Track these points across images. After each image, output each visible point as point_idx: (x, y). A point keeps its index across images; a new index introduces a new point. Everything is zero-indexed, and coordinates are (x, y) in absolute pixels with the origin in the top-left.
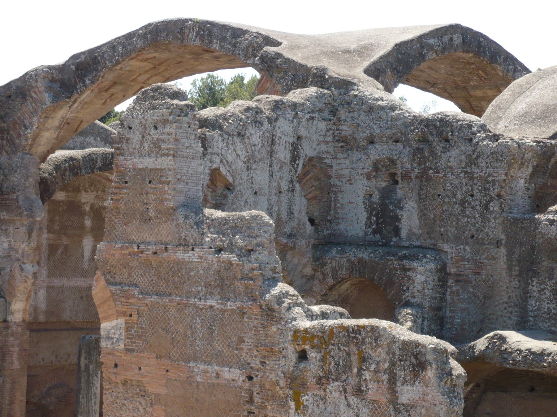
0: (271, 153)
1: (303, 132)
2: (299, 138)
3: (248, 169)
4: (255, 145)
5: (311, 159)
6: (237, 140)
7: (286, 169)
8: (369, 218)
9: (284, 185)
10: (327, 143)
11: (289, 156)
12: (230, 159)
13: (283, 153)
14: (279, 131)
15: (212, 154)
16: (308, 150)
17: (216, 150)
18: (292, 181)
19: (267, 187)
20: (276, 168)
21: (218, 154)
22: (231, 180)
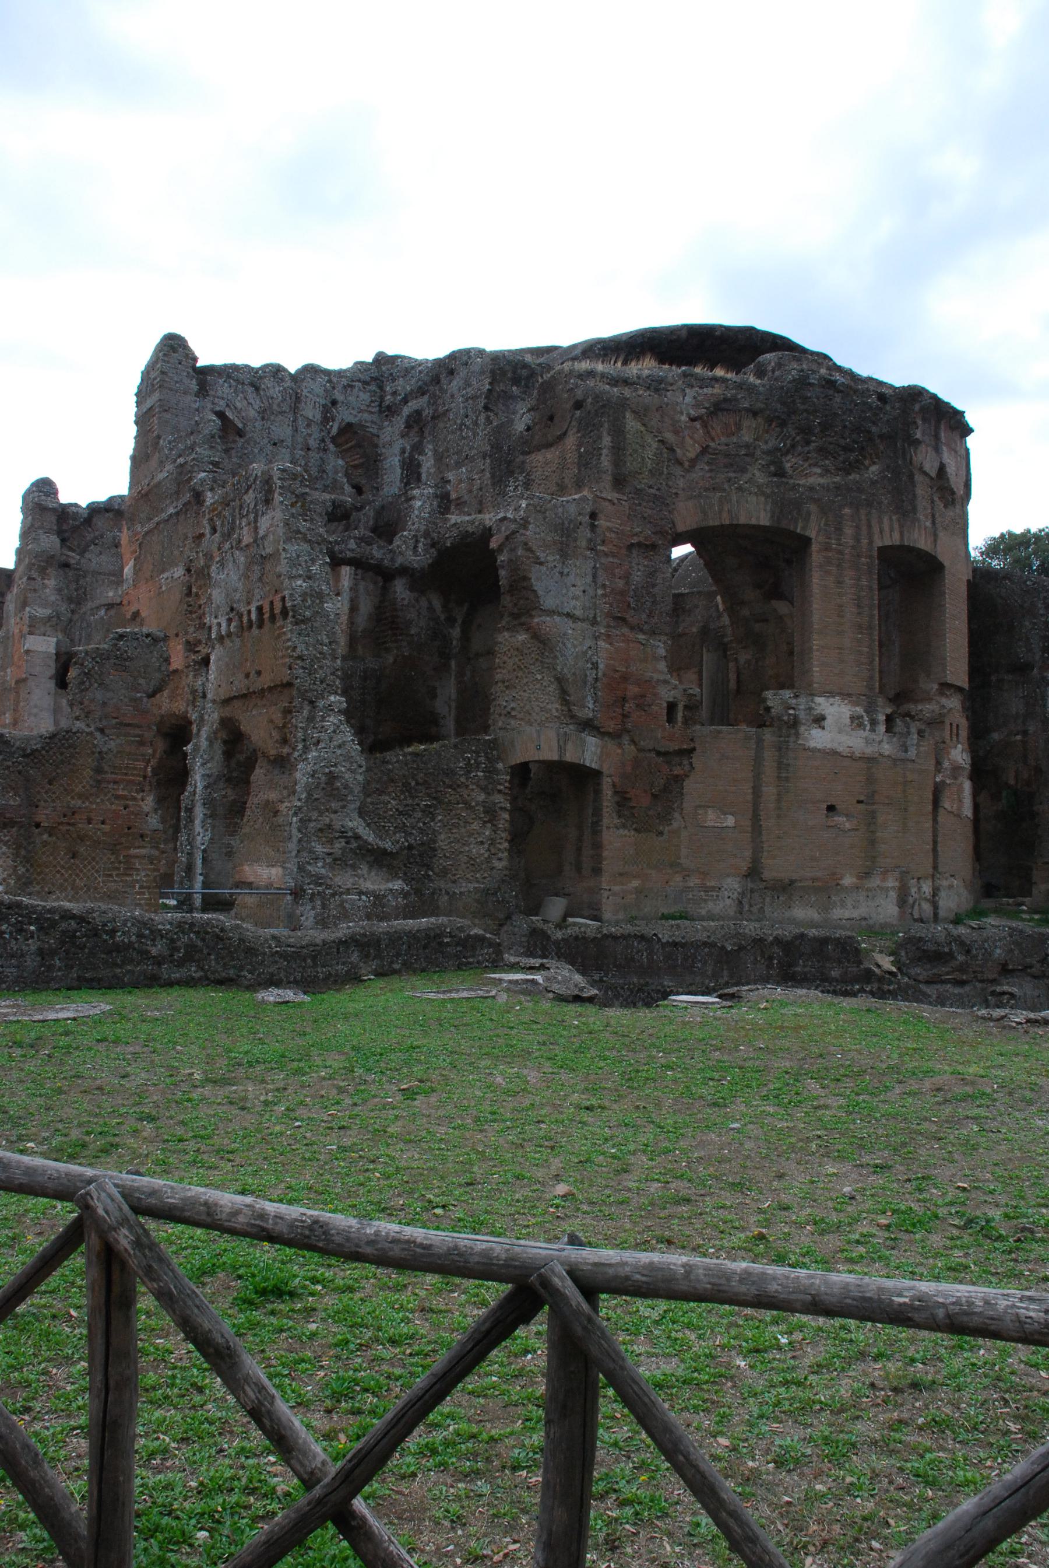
0: (295, 409)
1: (339, 396)
2: (334, 403)
3: (263, 419)
4: (272, 398)
5: (350, 425)
6: (250, 390)
7: (315, 429)
8: (402, 474)
9: (313, 443)
10: (372, 413)
11: (318, 417)
12: (239, 405)
13: (311, 411)
14: (305, 391)
15: (214, 396)
16: (344, 415)
17: (220, 393)
18: (323, 441)
19: (289, 440)
20: (301, 423)
21: (223, 399)
22: (240, 426)
